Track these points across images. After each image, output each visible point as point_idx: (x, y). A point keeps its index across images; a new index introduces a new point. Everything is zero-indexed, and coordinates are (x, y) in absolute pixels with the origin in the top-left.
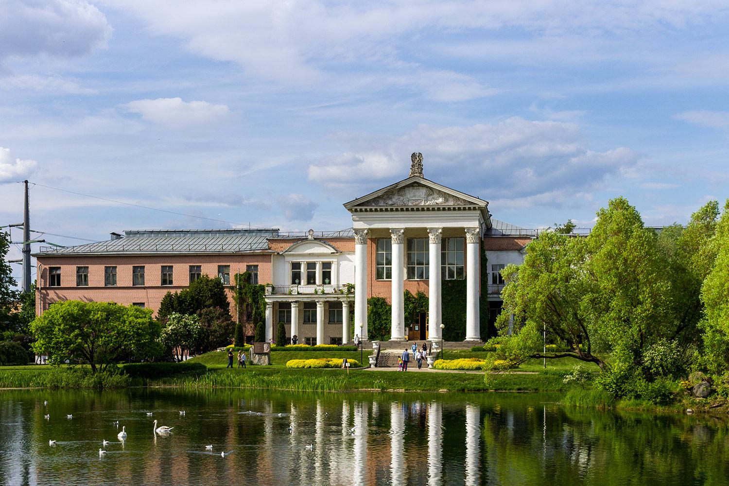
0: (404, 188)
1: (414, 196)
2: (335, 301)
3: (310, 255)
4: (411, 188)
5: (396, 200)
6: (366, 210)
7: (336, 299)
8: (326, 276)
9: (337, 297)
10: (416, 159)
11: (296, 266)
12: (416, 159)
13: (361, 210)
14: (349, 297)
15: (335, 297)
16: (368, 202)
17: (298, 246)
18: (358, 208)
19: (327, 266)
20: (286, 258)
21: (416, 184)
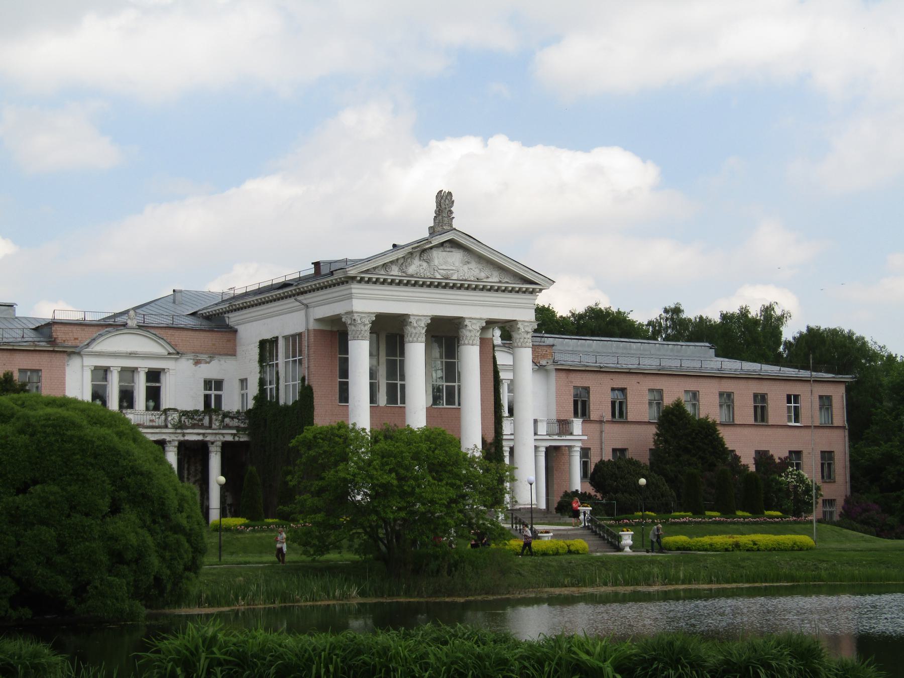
0: (431, 248)
1: (446, 263)
2: (198, 441)
3: (131, 355)
4: (442, 249)
5: (416, 267)
6: (377, 281)
7: (200, 438)
8: (154, 394)
9: (204, 434)
10: (444, 202)
11: (102, 373)
12: (444, 202)
13: (369, 281)
14: (223, 434)
15: (199, 434)
16: (375, 268)
17: (153, 339)
18: (367, 276)
19: (154, 376)
20: (85, 359)
21: (447, 244)
